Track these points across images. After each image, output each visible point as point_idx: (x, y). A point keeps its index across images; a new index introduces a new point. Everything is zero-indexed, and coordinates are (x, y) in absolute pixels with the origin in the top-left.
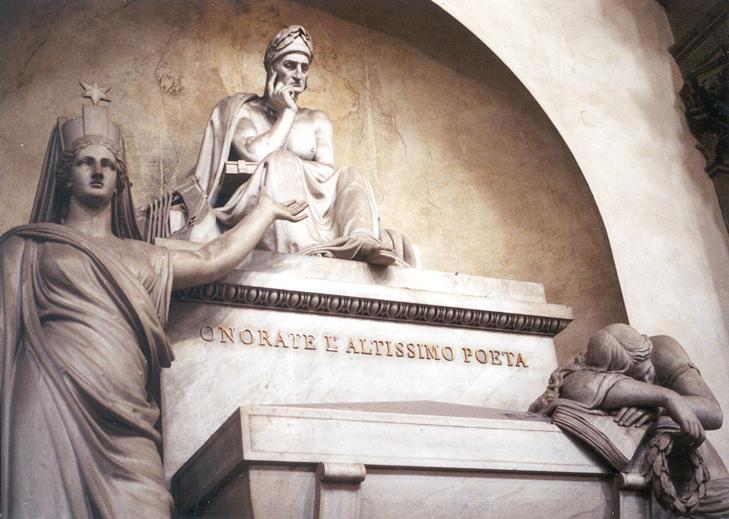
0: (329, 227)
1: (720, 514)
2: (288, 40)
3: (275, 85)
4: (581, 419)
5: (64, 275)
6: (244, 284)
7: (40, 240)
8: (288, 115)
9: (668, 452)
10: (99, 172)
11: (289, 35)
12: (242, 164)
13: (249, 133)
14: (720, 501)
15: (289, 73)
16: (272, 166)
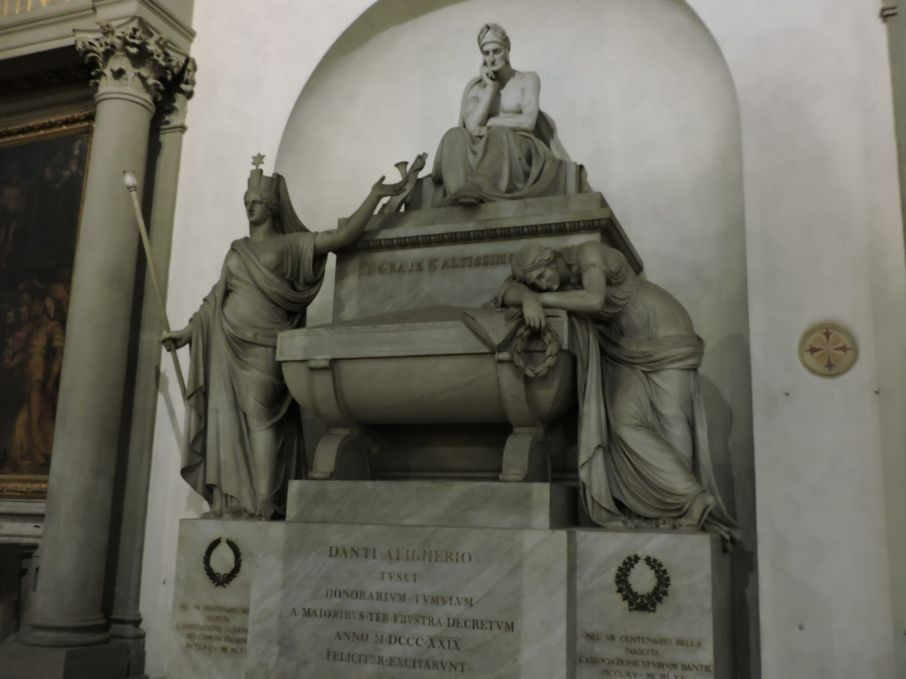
1: (652, 364)
2: (481, 36)
4: (473, 319)
9: (523, 337)
13: (470, 108)
14: (651, 355)
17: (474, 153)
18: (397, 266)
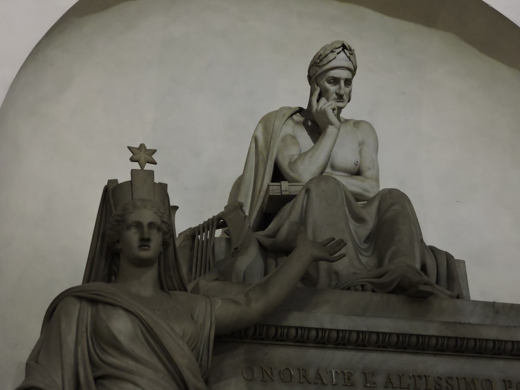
0: (369, 254)
2: (331, 56)
3: (318, 101)
5: (115, 338)
6: (284, 324)
7: (93, 302)
8: (331, 130)
10: (146, 236)
11: (332, 52)
12: (285, 185)
15: (332, 88)
16: (314, 193)
17: (360, 220)
18: (312, 374)
